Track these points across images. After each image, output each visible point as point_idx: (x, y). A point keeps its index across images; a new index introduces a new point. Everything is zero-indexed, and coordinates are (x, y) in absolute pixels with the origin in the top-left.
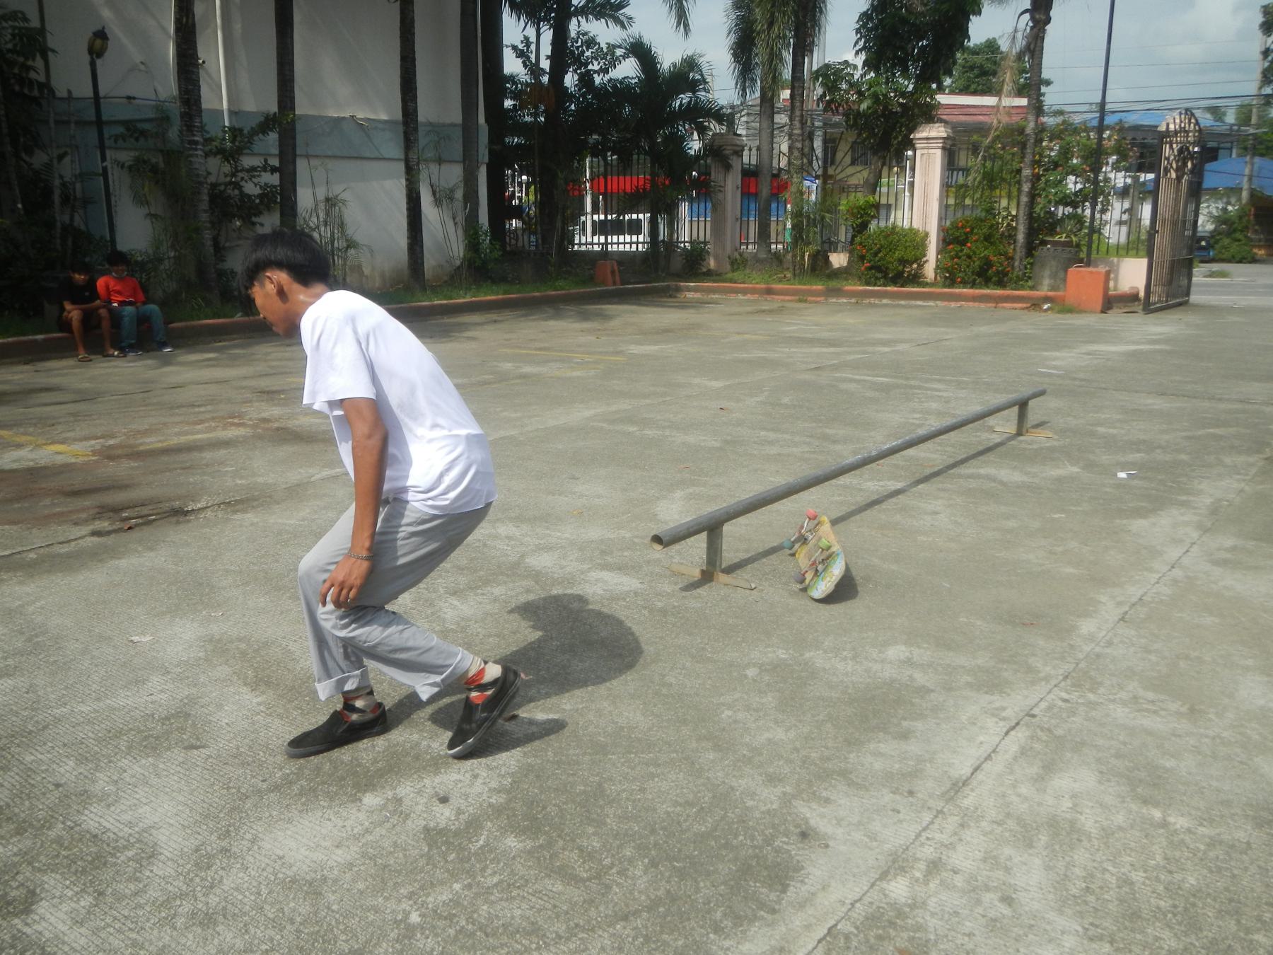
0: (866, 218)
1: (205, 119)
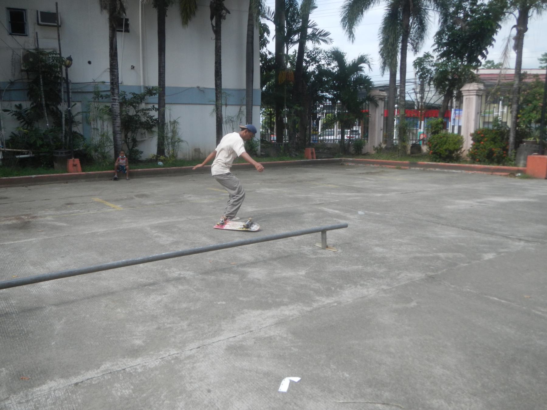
0: (437, 129)
1: (121, 89)
